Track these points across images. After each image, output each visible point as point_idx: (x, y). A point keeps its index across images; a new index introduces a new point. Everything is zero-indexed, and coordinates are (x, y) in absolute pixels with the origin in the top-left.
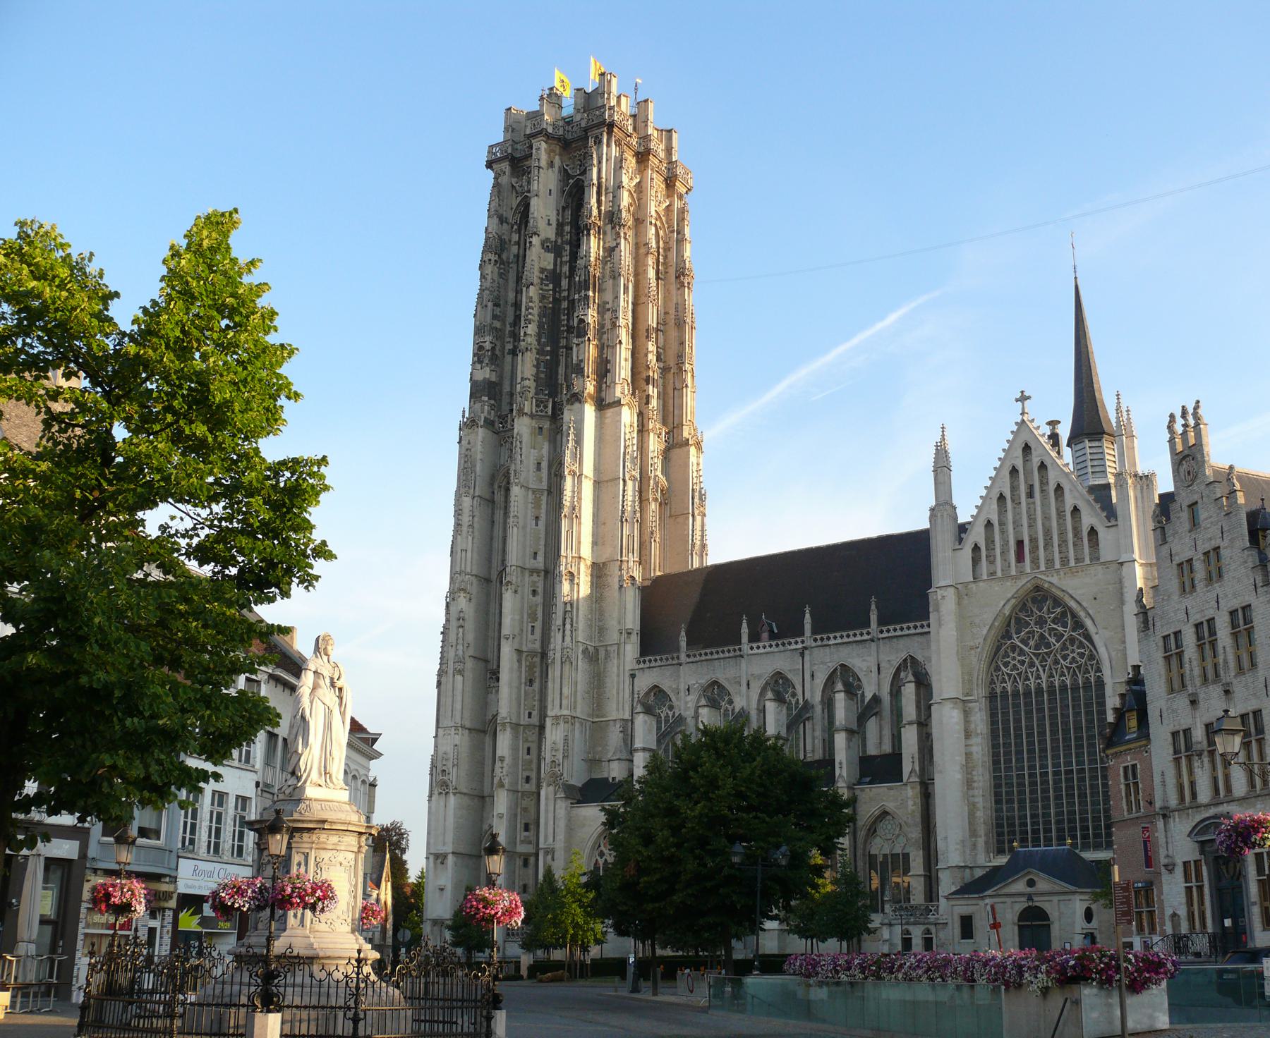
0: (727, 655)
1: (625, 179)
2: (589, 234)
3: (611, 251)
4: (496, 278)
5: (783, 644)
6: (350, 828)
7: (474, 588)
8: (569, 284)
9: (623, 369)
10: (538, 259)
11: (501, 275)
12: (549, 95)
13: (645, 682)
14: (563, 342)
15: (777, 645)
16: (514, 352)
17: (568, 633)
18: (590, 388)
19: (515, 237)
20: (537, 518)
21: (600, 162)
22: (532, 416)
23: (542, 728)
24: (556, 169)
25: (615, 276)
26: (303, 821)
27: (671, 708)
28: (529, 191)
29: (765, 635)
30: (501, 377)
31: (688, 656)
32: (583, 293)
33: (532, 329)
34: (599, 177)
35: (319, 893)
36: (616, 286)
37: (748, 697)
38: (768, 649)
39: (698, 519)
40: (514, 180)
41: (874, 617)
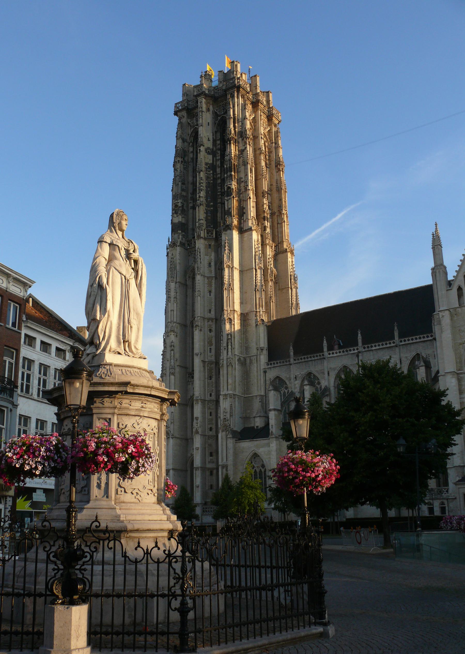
0: (316, 358)
1: (247, 114)
2: (230, 143)
3: (242, 152)
4: (182, 170)
5: (347, 351)
6: (154, 393)
7: (178, 329)
8: (222, 169)
9: (252, 212)
10: (204, 158)
11: (185, 169)
12: (205, 75)
13: (271, 374)
14: (219, 200)
15: (343, 352)
16: (194, 208)
17: (230, 350)
18: (235, 222)
19: (191, 149)
20: (210, 292)
21: (234, 106)
22: (205, 239)
23: (217, 402)
24: (211, 112)
25: (245, 164)
26: (104, 384)
27: (286, 388)
28: (197, 125)
29: (336, 347)
30: (187, 220)
31: (295, 360)
32: (229, 174)
33: (203, 194)
34: (234, 114)
35: (131, 449)
36: (246, 169)
37: (329, 380)
38: (338, 354)
39: (294, 290)
40: (189, 120)
41: (396, 334)
